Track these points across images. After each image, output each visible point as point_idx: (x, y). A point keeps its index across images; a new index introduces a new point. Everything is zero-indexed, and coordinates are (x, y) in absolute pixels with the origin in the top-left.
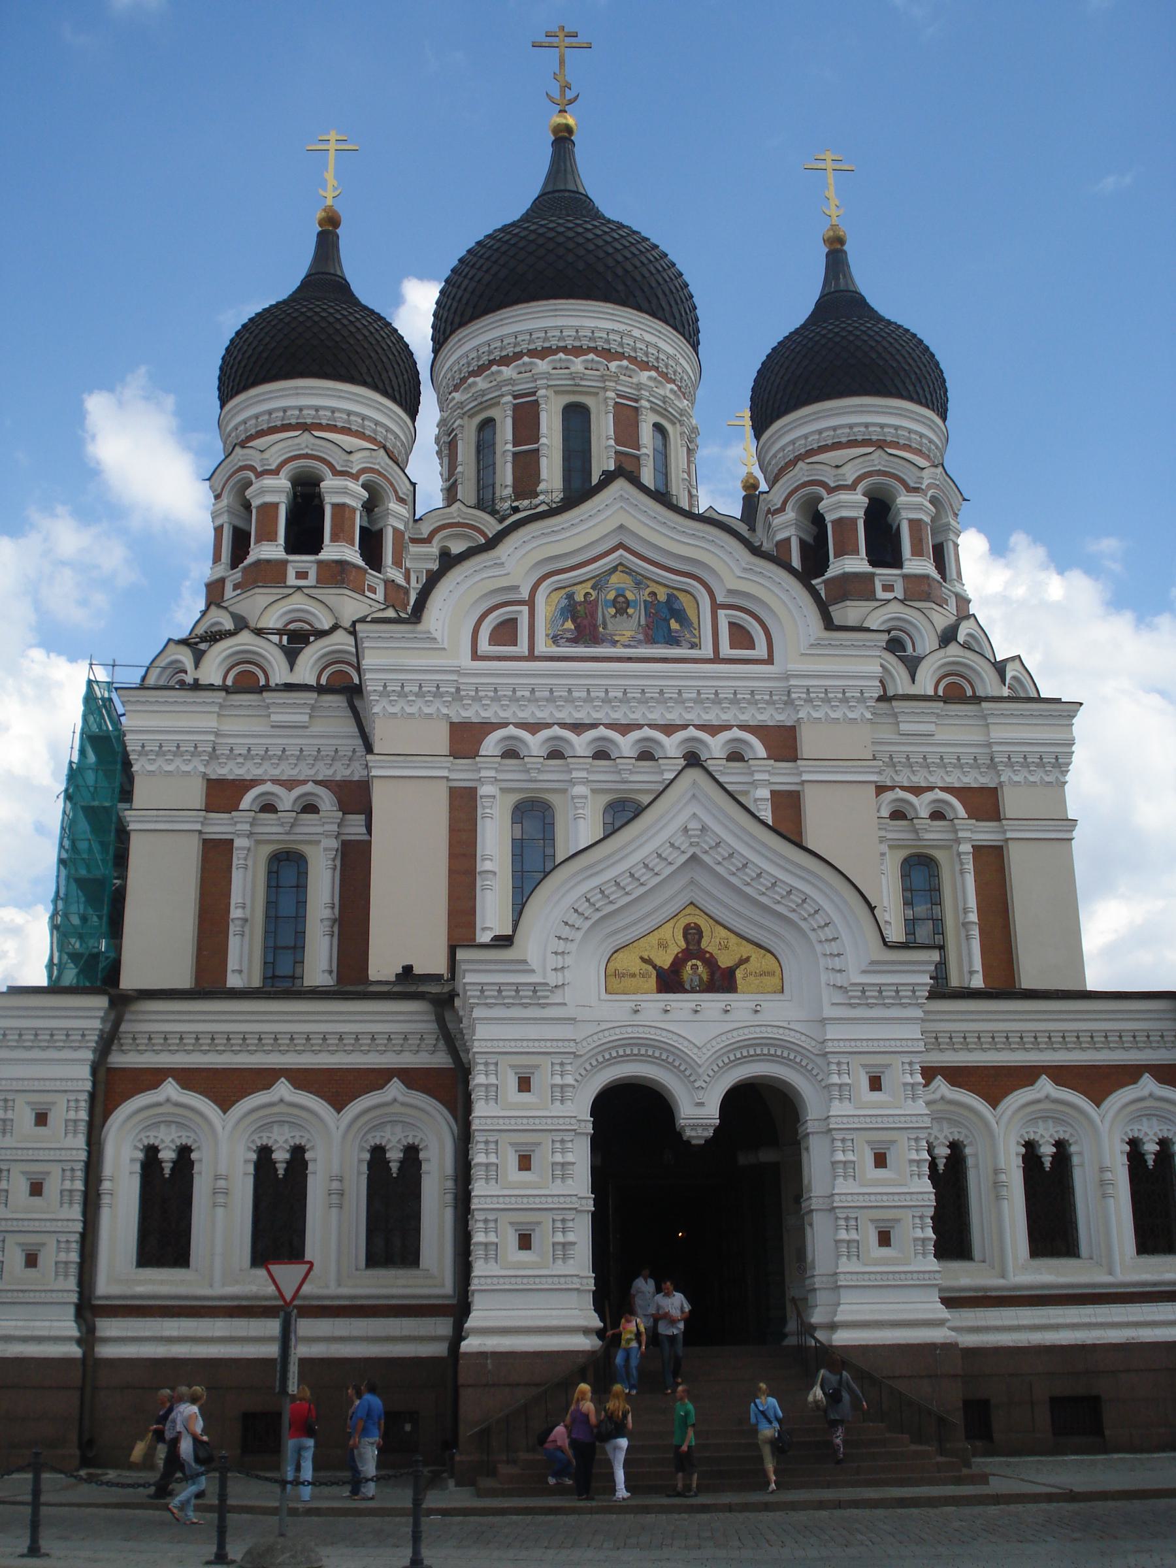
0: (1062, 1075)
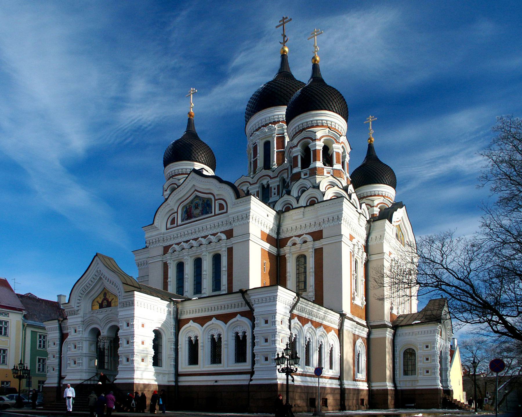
0: (218, 317)
